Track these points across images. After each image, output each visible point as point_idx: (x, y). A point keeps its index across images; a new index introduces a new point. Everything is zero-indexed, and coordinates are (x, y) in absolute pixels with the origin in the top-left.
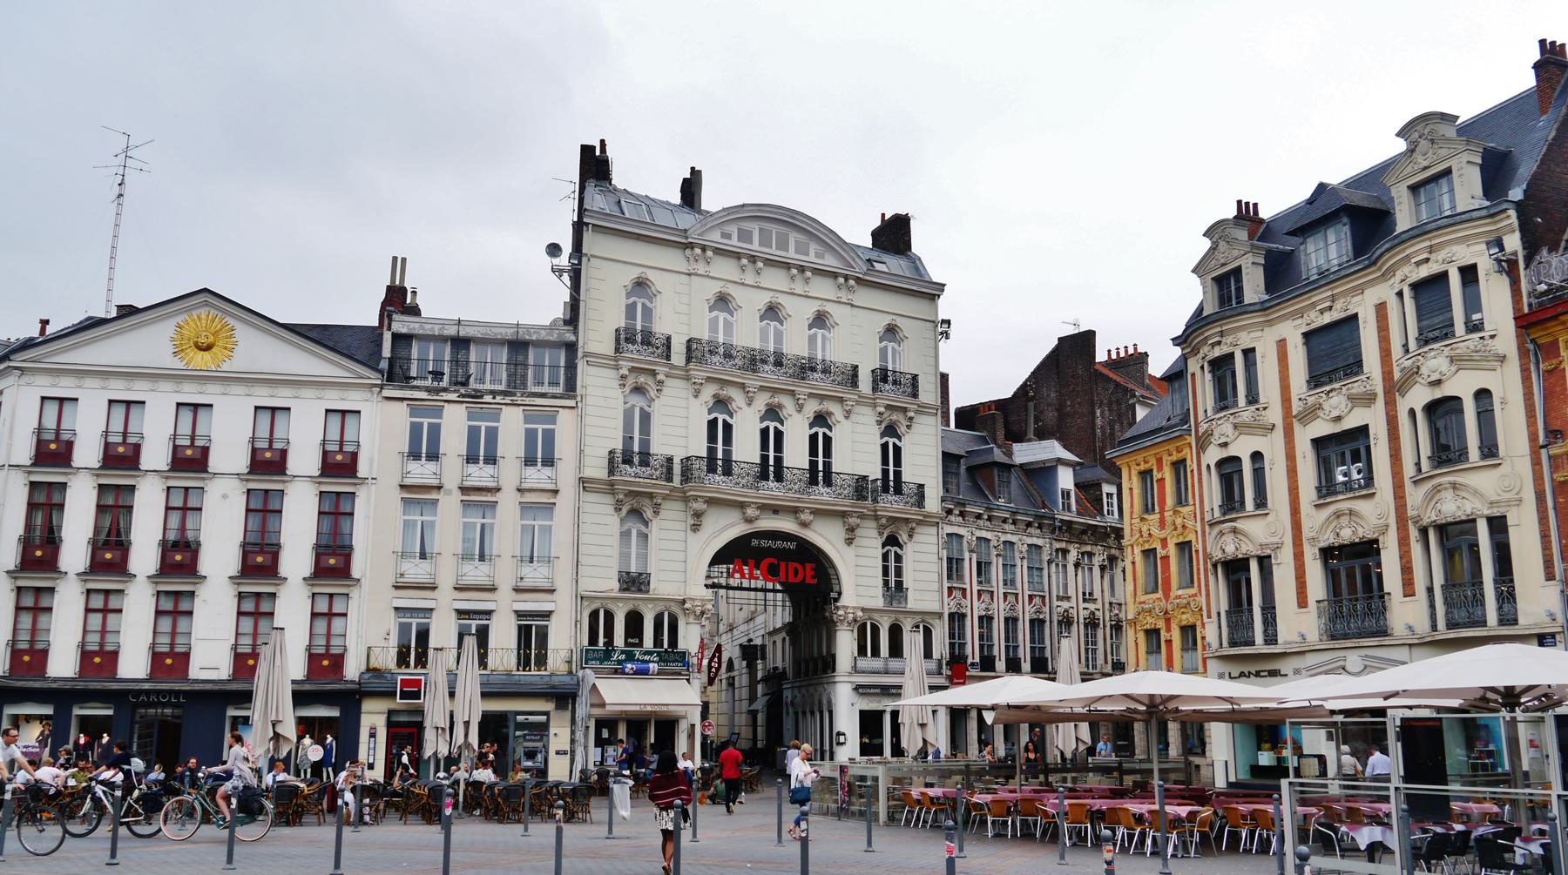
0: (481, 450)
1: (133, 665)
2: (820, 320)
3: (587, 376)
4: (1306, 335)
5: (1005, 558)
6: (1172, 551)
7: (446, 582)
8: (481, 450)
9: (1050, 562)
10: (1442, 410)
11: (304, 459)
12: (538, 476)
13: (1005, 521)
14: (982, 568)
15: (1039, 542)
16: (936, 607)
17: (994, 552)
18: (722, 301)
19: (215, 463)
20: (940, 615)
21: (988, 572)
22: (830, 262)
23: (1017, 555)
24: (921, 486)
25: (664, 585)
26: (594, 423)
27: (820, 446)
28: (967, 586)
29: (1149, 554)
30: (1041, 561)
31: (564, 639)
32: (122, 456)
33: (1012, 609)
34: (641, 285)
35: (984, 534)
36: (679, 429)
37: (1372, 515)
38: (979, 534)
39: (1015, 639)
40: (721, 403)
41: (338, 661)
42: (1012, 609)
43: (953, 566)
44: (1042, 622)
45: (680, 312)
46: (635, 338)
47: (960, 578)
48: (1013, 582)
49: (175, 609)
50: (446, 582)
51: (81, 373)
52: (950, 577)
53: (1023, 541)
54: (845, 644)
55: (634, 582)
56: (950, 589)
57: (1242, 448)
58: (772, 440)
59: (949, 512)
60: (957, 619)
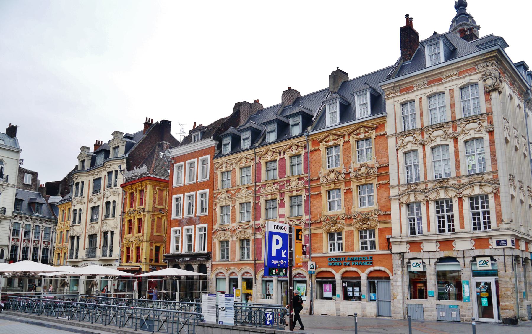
4: (94, 180)
5: (36, 230)
6: (65, 232)
9: (53, 232)
10: (108, 203)
13: (37, 219)
14: (26, 233)
15: (50, 226)
16: (7, 244)
17: (32, 228)
20: (8, 246)
21: (29, 234)
23: (41, 229)
24: (5, 208)
28: (20, 238)
29: (61, 232)
30: (50, 232)
33: (36, 245)
35: (28, 223)
38: (26, 223)
39: (37, 254)
42: (36, 245)
43: (15, 232)
44: (48, 249)
47: (18, 235)
48: (38, 237)
52: (13, 235)
53: (43, 226)
56: (13, 239)
57: (77, 208)
59: (16, 216)
60: (14, 249)
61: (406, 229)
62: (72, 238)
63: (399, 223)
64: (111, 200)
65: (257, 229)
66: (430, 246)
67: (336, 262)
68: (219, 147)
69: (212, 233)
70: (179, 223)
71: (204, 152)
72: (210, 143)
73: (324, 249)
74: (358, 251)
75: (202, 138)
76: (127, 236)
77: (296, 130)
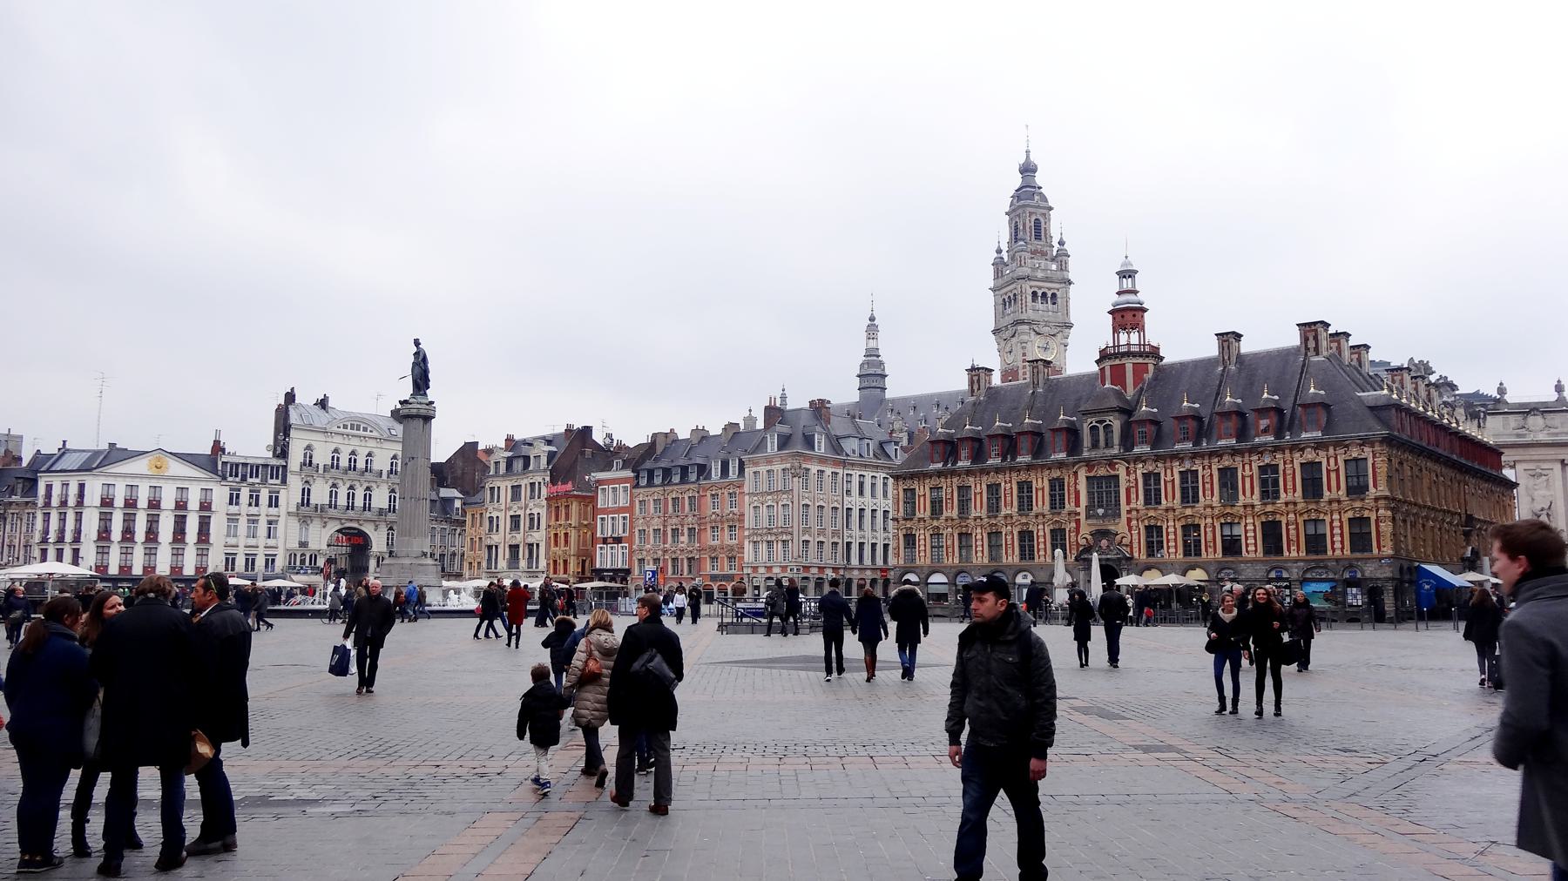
0: (255, 500)
1: (137, 570)
2: (369, 455)
3: (290, 477)
7: (242, 544)
8: (255, 500)
11: (193, 505)
12: (273, 511)
18: (336, 451)
19: (163, 505)
22: (375, 434)
25: (313, 546)
26: (290, 496)
27: (368, 498)
31: (280, 563)
32: (131, 504)
34: (309, 447)
36: (320, 495)
37: (518, 538)
40: (334, 485)
41: (205, 569)
45: (322, 457)
46: (308, 463)
49: (151, 553)
50: (242, 544)
51: (116, 475)
54: (372, 563)
55: (303, 544)
57: (494, 515)
58: (351, 497)
61: (752, 558)
62: (490, 547)
63: (748, 554)
64: (535, 511)
65: (665, 551)
66: (762, 570)
67: (714, 578)
68: (637, 477)
69: (631, 552)
70: (605, 541)
71: (625, 480)
72: (629, 474)
73: (708, 569)
74: (727, 571)
75: (623, 468)
76: (553, 549)
77: (693, 477)
